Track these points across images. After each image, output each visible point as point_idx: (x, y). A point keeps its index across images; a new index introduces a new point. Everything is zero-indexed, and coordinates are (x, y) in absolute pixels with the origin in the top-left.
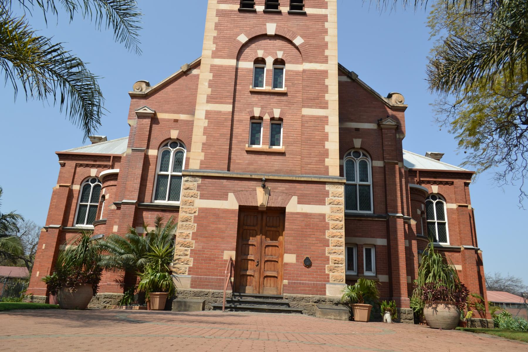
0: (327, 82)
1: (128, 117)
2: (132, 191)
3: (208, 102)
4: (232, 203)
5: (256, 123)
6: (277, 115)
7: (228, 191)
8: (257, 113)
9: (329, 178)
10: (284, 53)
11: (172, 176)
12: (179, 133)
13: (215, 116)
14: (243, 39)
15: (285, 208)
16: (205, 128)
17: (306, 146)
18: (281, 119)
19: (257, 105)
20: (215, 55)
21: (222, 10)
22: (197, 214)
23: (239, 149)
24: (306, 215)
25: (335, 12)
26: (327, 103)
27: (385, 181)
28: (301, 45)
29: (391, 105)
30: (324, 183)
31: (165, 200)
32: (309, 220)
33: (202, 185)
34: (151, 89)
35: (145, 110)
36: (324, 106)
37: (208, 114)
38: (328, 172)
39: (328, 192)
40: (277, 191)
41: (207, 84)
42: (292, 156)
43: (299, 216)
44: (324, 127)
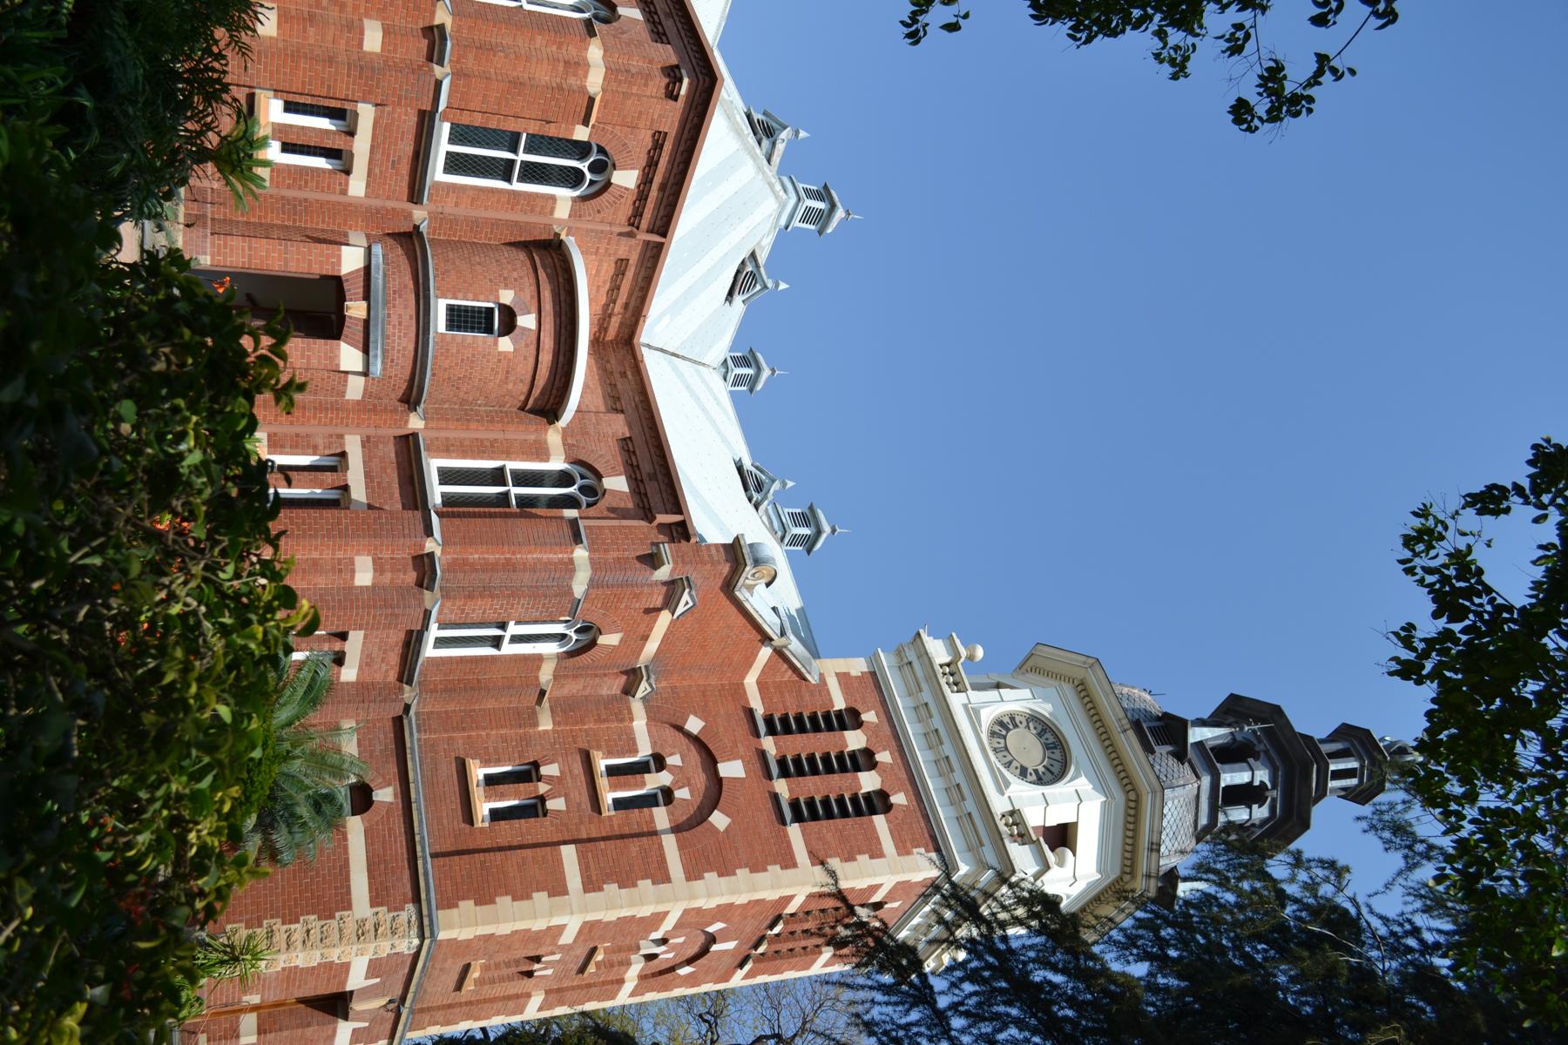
5: (529, 774)
6: (551, 805)
8: (544, 770)
14: (694, 725)
28: (713, 828)
30: (417, 899)
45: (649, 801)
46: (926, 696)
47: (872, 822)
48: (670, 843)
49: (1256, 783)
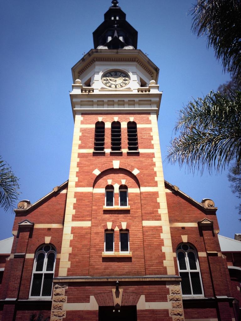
0: (159, 200)
1: (12, 229)
2: (13, 290)
3: (73, 220)
4: (92, 305)
6: (124, 226)
7: (89, 294)
8: (109, 226)
9: (168, 278)
10: (126, 181)
11: (45, 274)
12: (51, 239)
13: (79, 231)
14: (97, 172)
15: (136, 306)
16: (71, 241)
17: (148, 251)
18: (127, 230)
19: (109, 220)
20: (77, 185)
21: (82, 154)
22: (65, 317)
23: (97, 257)
24: (153, 312)
25: (160, 150)
26: (160, 216)
28: (138, 174)
29: (205, 208)
31: (39, 295)
32: (155, 316)
33: (69, 290)
34: (31, 207)
35: (26, 222)
36: (158, 218)
37: (74, 230)
38: (167, 272)
39: (168, 289)
40: (128, 291)
41: (72, 207)
42: (138, 260)
43: (147, 313)
44: (160, 235)
46: (95, 100)
47: (139, 128)
48: (144, 189)
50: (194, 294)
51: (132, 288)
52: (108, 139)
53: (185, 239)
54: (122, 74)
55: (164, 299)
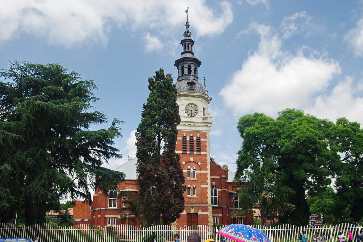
6: (194, 186)
15: (198, 213)
24: (203, 215)
27: (222, 196)
45: (194, 172)
49: (195, 68)
50: (214, 205)
51: (197, 208)
52: (188, 147)
53: (214, 183)
54: (195, 106)
55: (207, 211)
